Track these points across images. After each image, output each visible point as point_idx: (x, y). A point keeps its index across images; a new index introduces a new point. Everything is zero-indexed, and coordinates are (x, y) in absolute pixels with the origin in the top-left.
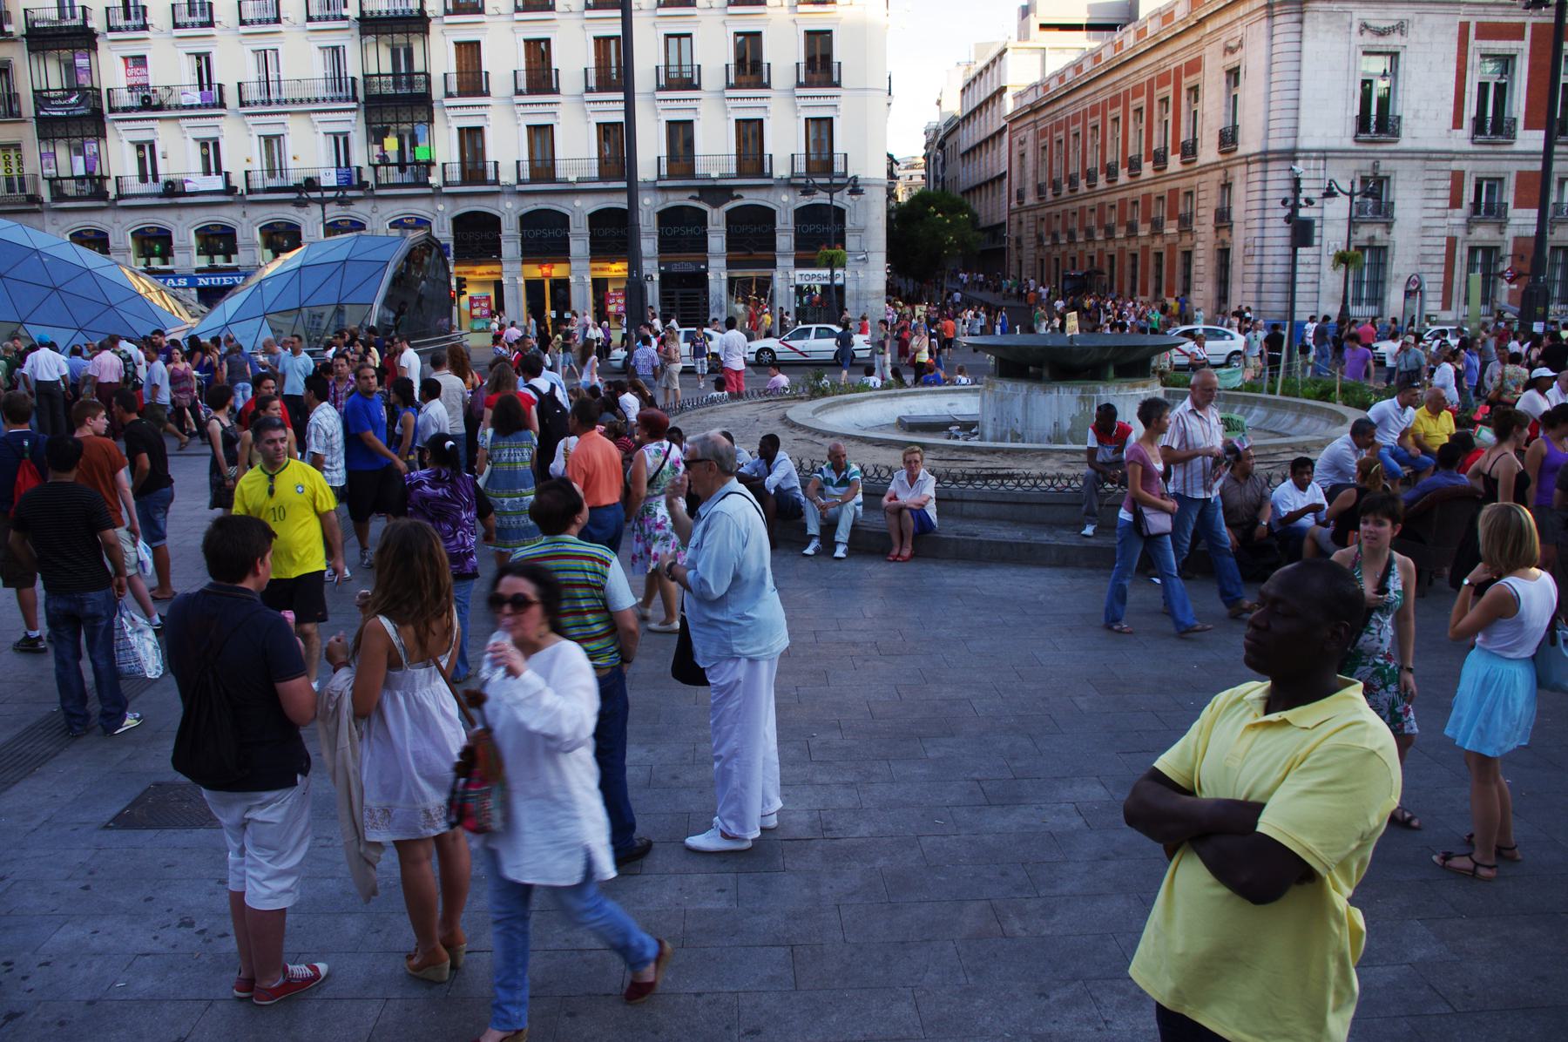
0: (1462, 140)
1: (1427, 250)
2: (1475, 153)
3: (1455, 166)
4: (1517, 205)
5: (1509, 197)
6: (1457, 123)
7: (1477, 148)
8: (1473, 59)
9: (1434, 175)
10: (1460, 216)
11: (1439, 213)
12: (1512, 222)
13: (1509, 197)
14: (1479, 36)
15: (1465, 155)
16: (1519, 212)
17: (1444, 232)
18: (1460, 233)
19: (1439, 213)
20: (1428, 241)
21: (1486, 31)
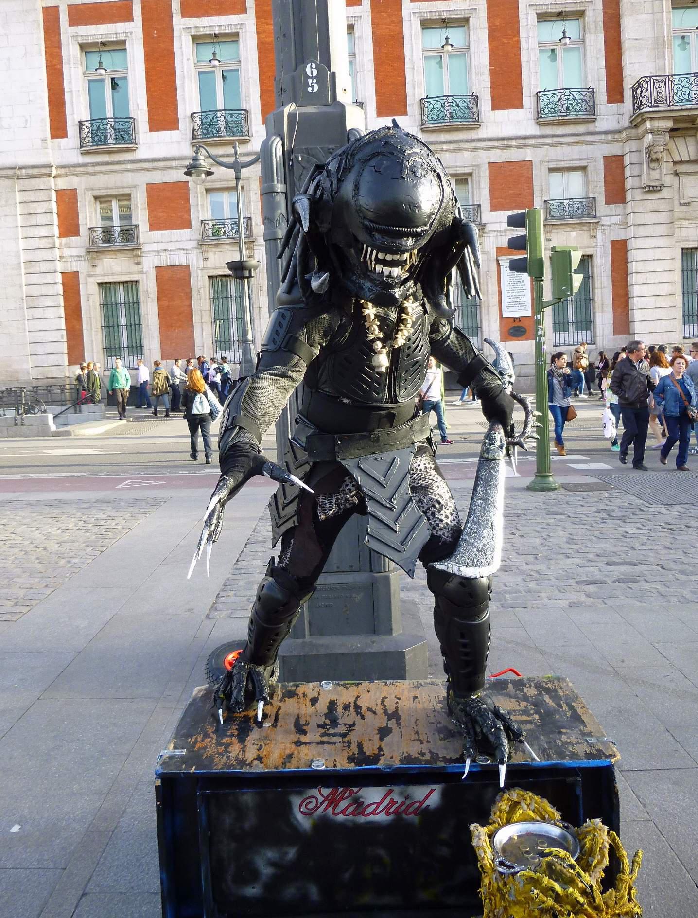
0: (66, 151)
1: (35, 290)
2: (85, 165)
3: (63, 184)
4: (155, 226)
5: (141, 217)
6: (58, 129)
7: (89, 159)
8: (70, 51)
9: (31, 196)
10: (77, 245)
11: (44, 243)
12: (146, 248)
13: (141, 217)
14: (73, 22)
15: (69, 168)
16: (158, 235)
17: (60, 267)
18: (81, 267)
19: (44, 243)
20: (35, 279)
21: (79, 16)
